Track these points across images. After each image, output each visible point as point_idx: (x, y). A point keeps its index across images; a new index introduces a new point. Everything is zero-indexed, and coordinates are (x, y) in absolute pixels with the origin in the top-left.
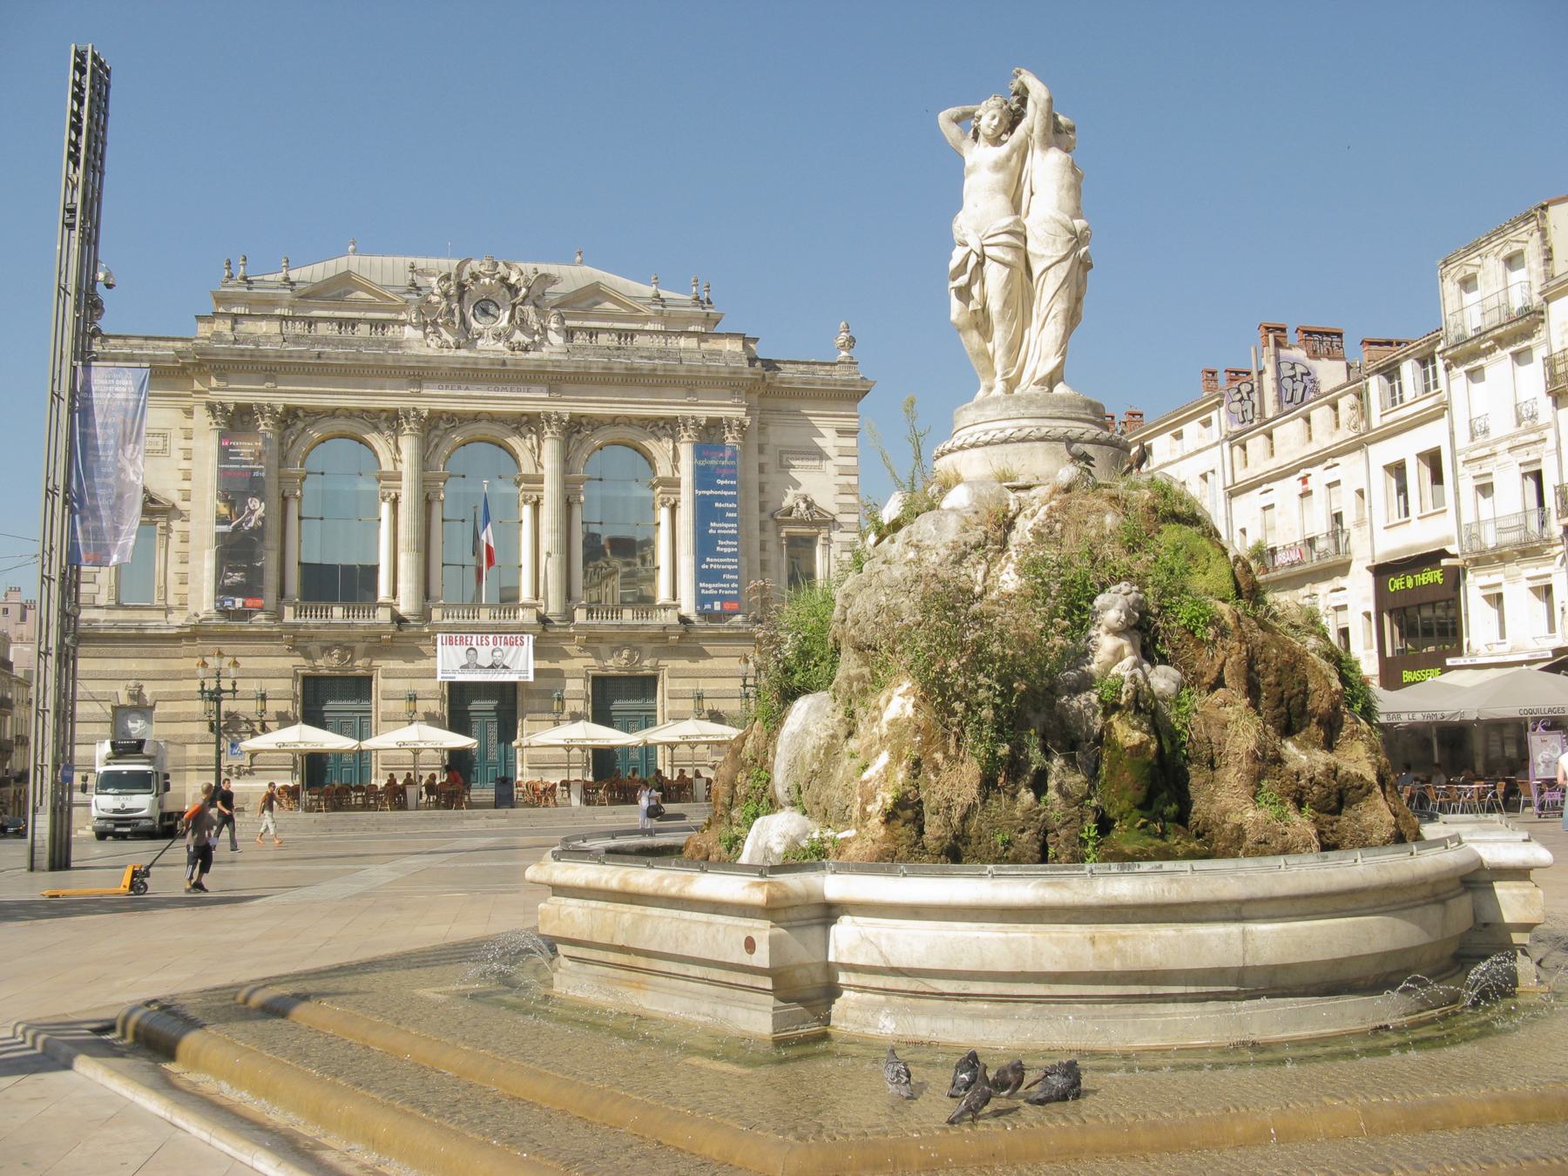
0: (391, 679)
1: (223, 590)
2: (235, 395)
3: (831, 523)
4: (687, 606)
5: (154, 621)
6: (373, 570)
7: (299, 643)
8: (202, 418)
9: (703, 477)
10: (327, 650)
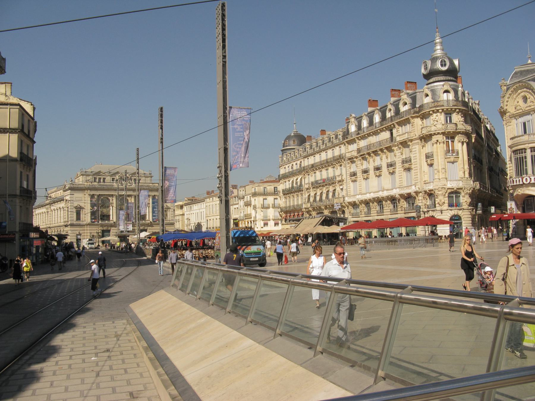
0: (113, 231)
1: (91, 219)
2: (93, 193)
3: (170, 208)
4: (151, 220)
5: (81, 223)
6: (109, 216)
7: (102, 225)
8: (87, 196)
9: (153, 203)
10: (105, 226)
